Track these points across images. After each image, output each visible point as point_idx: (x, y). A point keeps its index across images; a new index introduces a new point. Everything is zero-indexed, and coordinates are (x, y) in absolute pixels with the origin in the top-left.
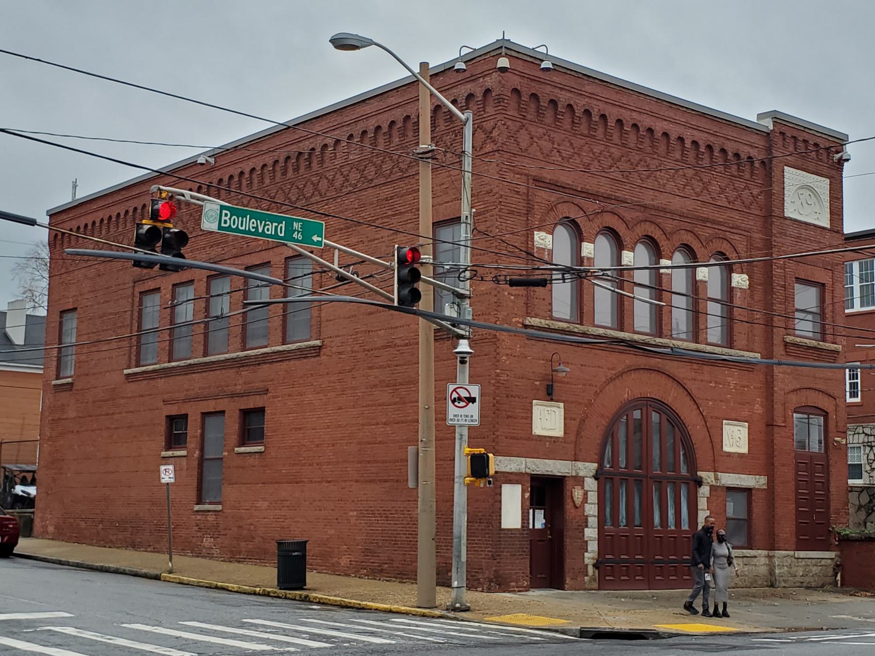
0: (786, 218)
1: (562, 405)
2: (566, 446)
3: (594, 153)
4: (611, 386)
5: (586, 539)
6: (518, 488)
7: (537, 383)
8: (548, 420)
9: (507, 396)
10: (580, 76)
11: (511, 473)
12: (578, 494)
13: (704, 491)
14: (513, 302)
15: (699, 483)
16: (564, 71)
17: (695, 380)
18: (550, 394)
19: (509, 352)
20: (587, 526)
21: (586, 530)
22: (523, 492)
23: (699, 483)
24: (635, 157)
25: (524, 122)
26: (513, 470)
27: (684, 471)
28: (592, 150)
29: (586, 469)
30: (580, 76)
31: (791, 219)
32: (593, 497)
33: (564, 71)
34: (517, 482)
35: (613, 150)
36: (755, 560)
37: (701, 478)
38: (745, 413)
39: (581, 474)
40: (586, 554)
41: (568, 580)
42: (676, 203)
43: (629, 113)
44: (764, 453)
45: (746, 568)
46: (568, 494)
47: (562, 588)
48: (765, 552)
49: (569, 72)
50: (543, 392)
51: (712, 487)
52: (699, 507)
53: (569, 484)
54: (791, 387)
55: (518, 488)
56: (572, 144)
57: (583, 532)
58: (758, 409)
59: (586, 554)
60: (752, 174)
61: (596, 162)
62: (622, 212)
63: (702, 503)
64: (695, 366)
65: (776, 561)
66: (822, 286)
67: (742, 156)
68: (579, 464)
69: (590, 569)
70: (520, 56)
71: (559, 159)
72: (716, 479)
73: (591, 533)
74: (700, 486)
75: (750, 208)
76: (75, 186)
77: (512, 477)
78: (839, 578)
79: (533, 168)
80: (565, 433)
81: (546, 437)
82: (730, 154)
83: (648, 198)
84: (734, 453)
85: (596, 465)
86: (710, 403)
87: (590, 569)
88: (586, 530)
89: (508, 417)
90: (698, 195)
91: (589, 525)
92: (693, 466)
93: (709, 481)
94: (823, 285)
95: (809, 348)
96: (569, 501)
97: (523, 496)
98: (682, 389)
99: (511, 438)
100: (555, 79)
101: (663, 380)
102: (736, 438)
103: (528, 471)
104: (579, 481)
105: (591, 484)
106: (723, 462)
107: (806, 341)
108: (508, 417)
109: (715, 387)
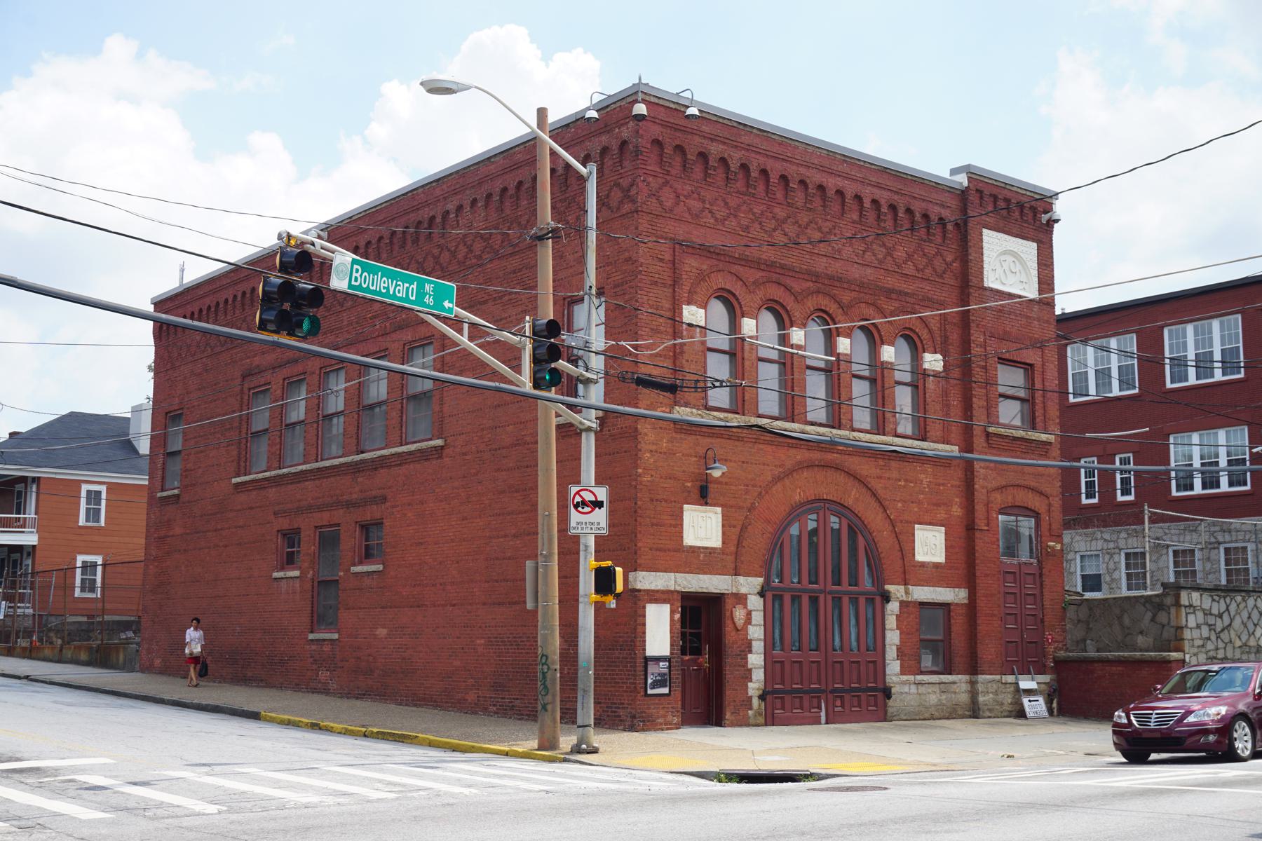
0: (985, 289)
1: (719, 510)
2: (728, 559)
3: (754, 214)
4: (779, 486)
5: (750, 666)
6: (666, 608)
8: (702, 527)
9: (652, 500)
11: (658, 591)
12: (739, 614)
13: (893, 607)
15: (886, 598)
18: (703, 496)
19: (654, 448)
20: (750, 652)
22: (672, 612)
23: (886, 598)
24: (804, 218)
25: (668, 178)
26: (660, 587)
27: (867, 583)
29: (749, 585)
31: (992, 290)
32: (758, 617)
34: (664, 601)
37: (889, 592)
38: (942, 515)
39: (743, 590)
40: (750, 685)
41: (728, 716)
42: (856, 272)
43: (794, 167)
44: (965, 561)
46: (728, 614)
47: (719, 723)
48: (967, 677)
50: (695, 494)
52: (887, 627)
53: (729, 602)
54: (994, 484)
55: (666, 608)
56: (726, 204)
57: (746, 659)
58: (957, 511)
59: (750, 685)
60: (944, 237)
61: (757, 226)
62: (788, 281)
63: (891, 622)
64: (881, 462)
65: (980, 687)
66: (1028, 368)
68: (741, 579)
69: (755, 702)
70: (661, 102)
71: (712, 221)
72: (907, 592)
73: (756, 659)
74: (888, 601)
75: (941, 277)
76: (182, 270)
77: (658, 595)
78: (1055, 705)
79: (681, 232)
83: (821, 265)
85: (761, 580)
87: (755, 702)
89: (653, 525)
90: (880, 262)
91: (754, 649)
92: (879, 579)
94: (1031, 365)
95: (1015, 439)
96: (728, 622)
97: (672, 619)
98: (864, 490)
100: (704, 128)
101: (841, 478)
102: (930, 545)
103: (678, 588)
104: (741, 599)
105: (755, 602)
106: (912, 572)
108: (653, 525)
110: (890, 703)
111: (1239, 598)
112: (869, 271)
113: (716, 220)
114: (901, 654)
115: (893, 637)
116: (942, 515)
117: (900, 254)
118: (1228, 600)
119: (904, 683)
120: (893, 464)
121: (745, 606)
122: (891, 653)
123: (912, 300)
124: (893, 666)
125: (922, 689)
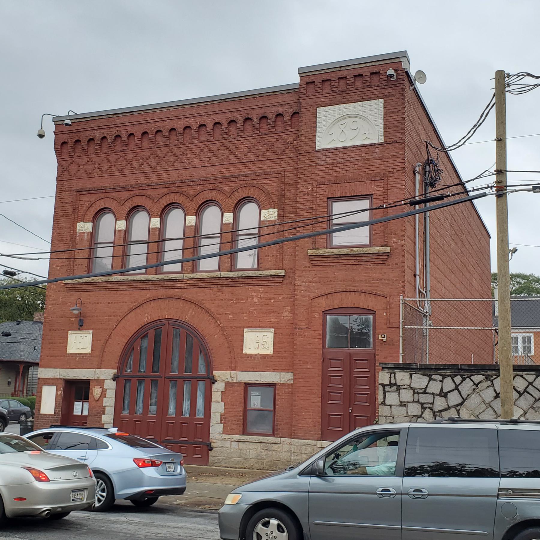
1: (91, 331)
5: (103, 422)
6: (54, 388)
7: (73, 319)
8: (80, 342)
10: (110, 116)
11: (49, 379)
13: (218, 388)
14: (59, 270)
16: (98, 118)
17: (215, 300)
19: (53, 302)
20: (104, 414)
21: (103, 416)
23: (213, 381)
25: (73, 159)
28: (126, 159)
29: (107, 375)
30: (110, 116)
32: (111, 393)
33: (98, 118)
35: (142, 154)
36: (277, 446)
39: (102, 377)
45: (264, 453)
49: (101, 117)
50: (76, 325)
51: (227, 384)
55: (54, 388)
57: (100, 418)
58: (286, 315)
61: (129, 166)
62: (149, 192)
63: (216, 396)
64: (215, 290)
67: (269, 116)
71: (100, 173)
74: (213, 383)
77: (49, 381)
79: (79, 184)
80: (92, 350)
81: (76, 354)
82: (255, 119)
83: (173, 177)
84: (256, 355)
86: (230, 316)
88: (103, 416)
91: (106, 412)
92: (210, 368)
93: (224, 378)
98: (200, 310)
99: (51, 356)
100: (92, 125)
101: (180, 304)
102: (258, 342)
103: (61, 377)
104: (100, 382)
105: (111, 386)
107: (365, 249)
109: (236, 303)
110: (211, 453)
111: (477, 378)
112: (213, 168)
113: (102, 171)
114: (223, 419)
115: (218, 407)
116: (272, 319)
117: (243, 149)
118: (458, 379)
119: (226, 440)
120: (226, 290)
121: (102, 387)
122: (215, 418)
123: (250, 178)
124: (216, 428)
125: (242, 445)
